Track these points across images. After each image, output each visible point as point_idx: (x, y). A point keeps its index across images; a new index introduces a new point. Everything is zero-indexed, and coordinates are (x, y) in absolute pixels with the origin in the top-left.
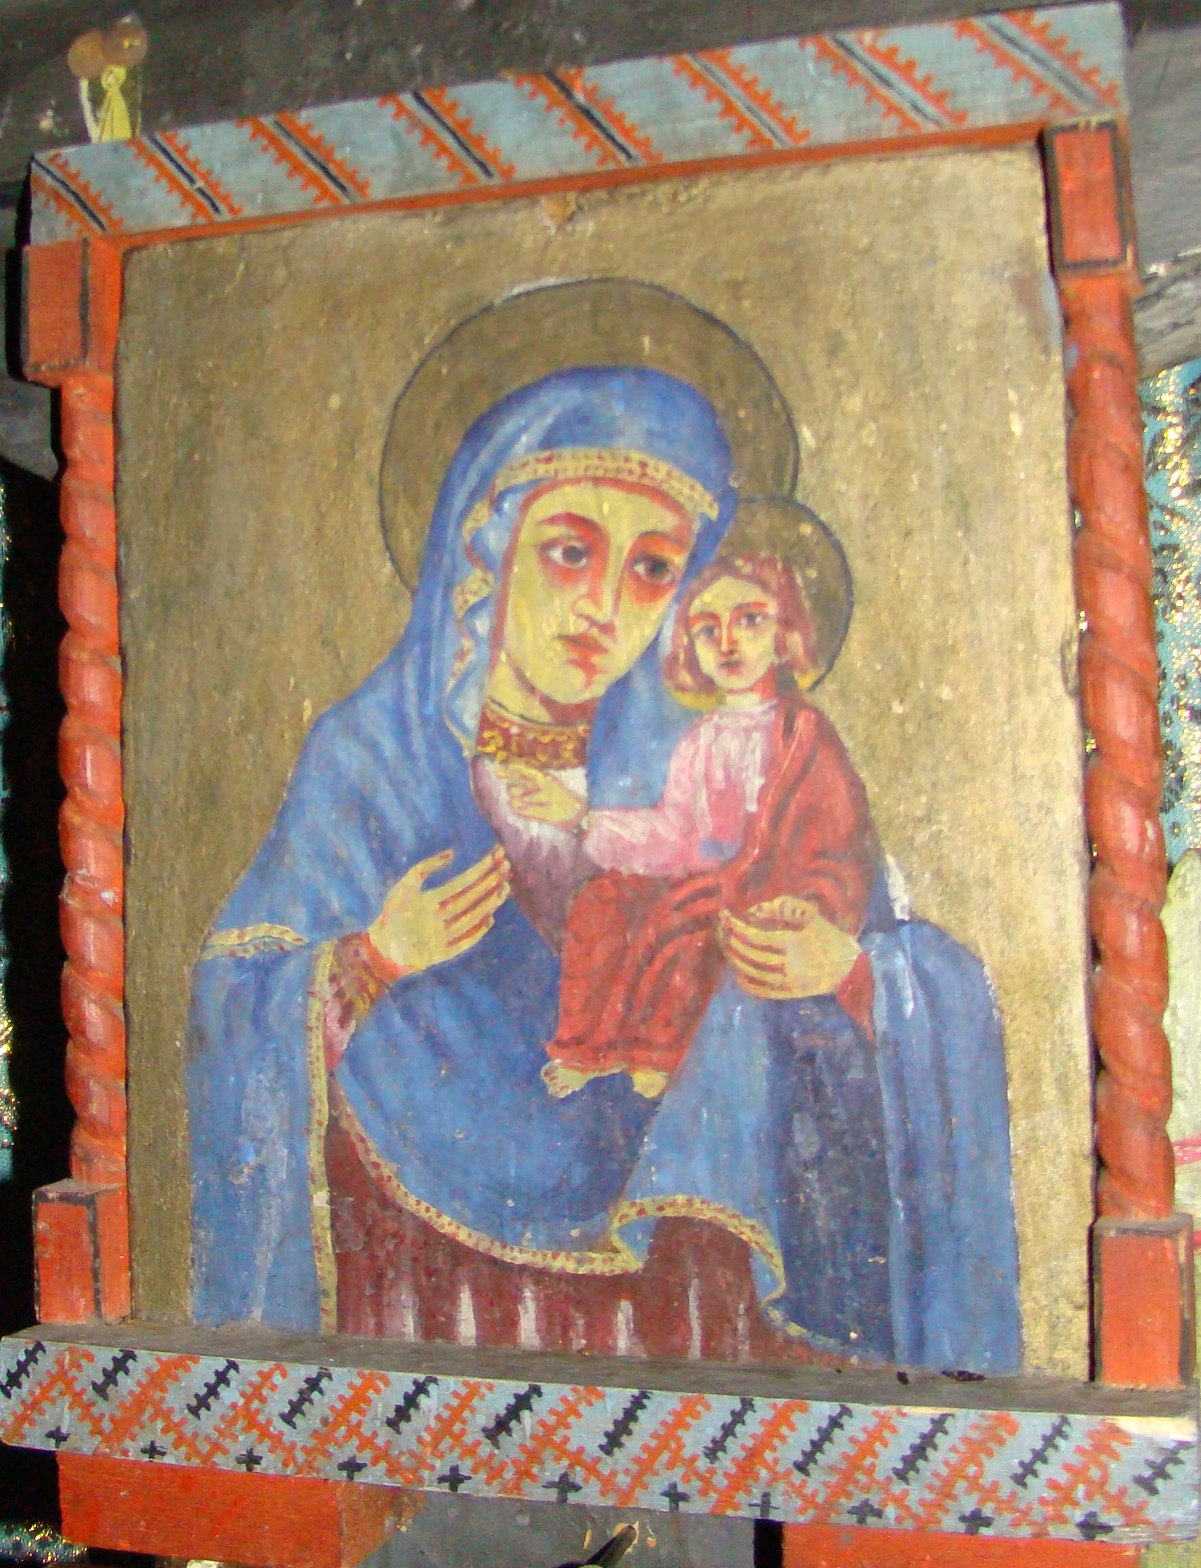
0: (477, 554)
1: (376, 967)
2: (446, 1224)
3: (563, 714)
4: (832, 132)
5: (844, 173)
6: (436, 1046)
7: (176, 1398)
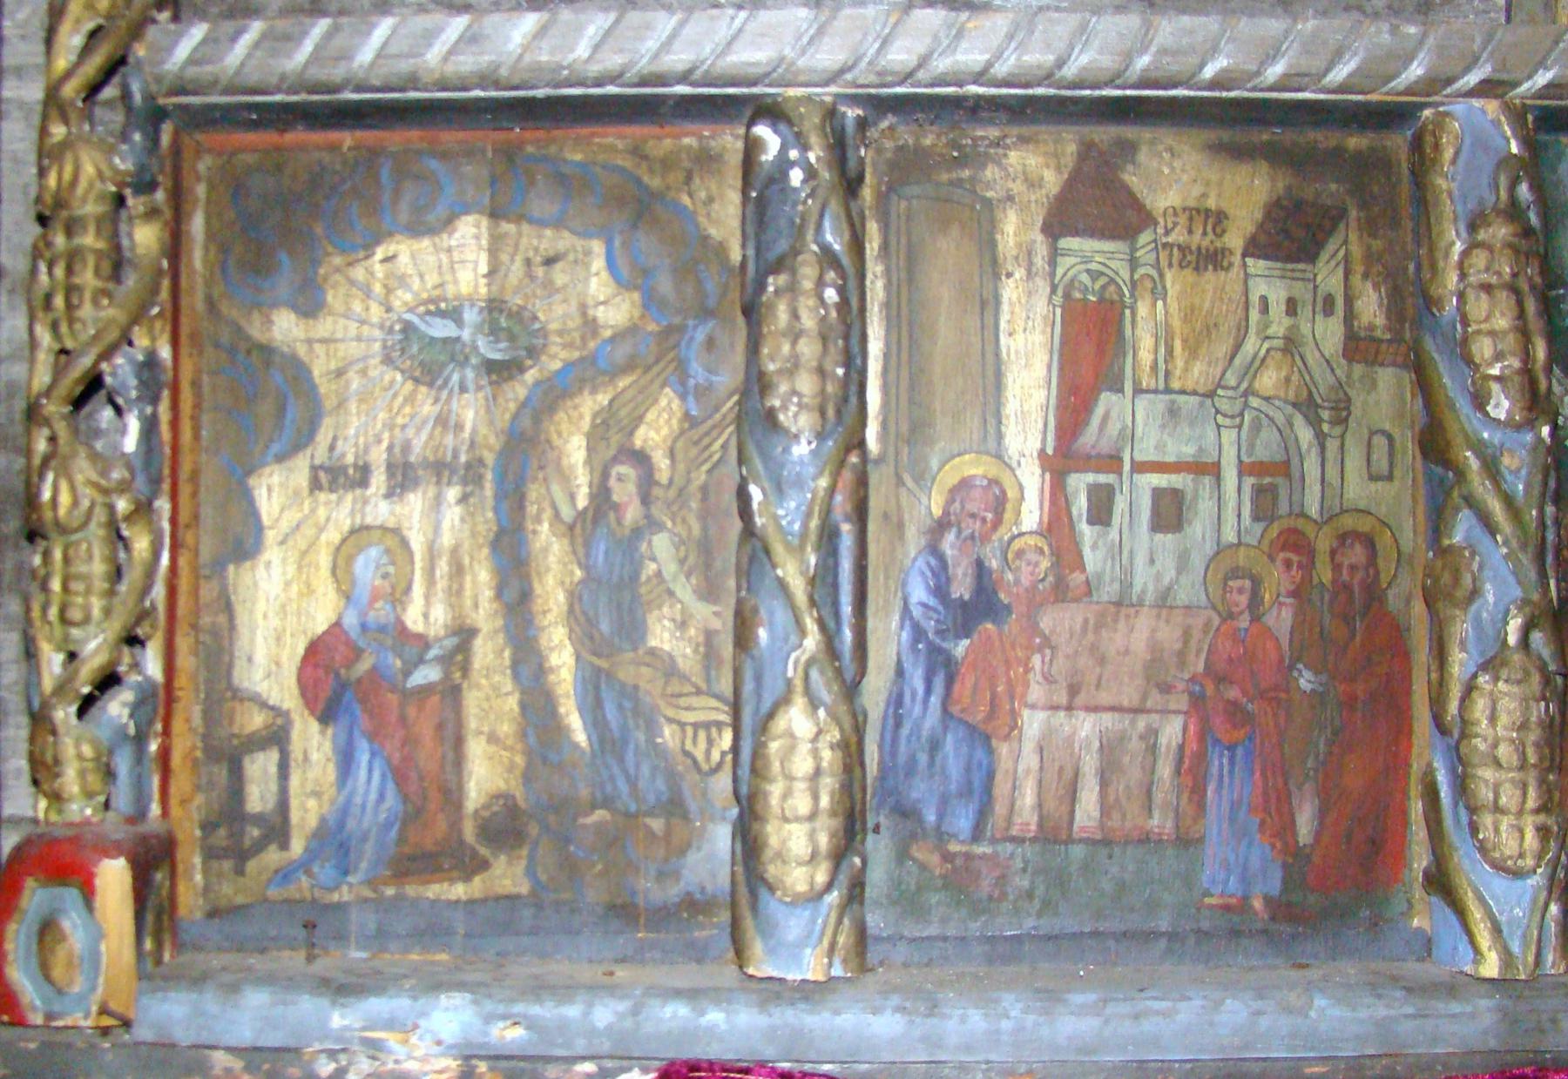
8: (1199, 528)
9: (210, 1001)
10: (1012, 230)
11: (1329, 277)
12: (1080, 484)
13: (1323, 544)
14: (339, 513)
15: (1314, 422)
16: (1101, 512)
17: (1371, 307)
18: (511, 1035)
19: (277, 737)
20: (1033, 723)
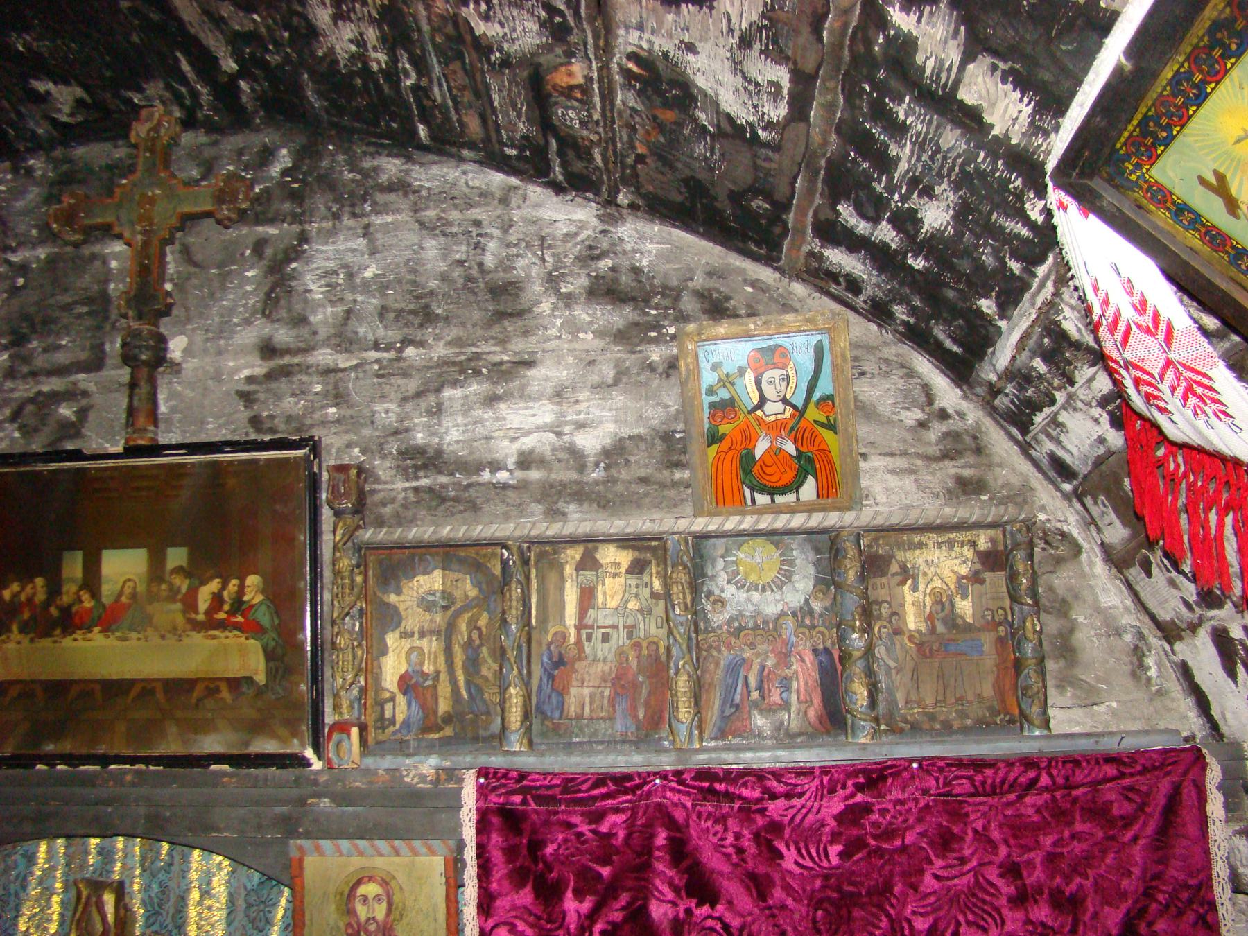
8: (613, 642)
9: (378, 759)
10: (569, 570)
11: (646, 578)
12: (584, 632)
13: (644, 645)
14: (407, 644)
15: (642, 614)
16: (589, 639)
17: (657, 585)
18: (447, 764)
19: (392, 699)
20: (573, 691)
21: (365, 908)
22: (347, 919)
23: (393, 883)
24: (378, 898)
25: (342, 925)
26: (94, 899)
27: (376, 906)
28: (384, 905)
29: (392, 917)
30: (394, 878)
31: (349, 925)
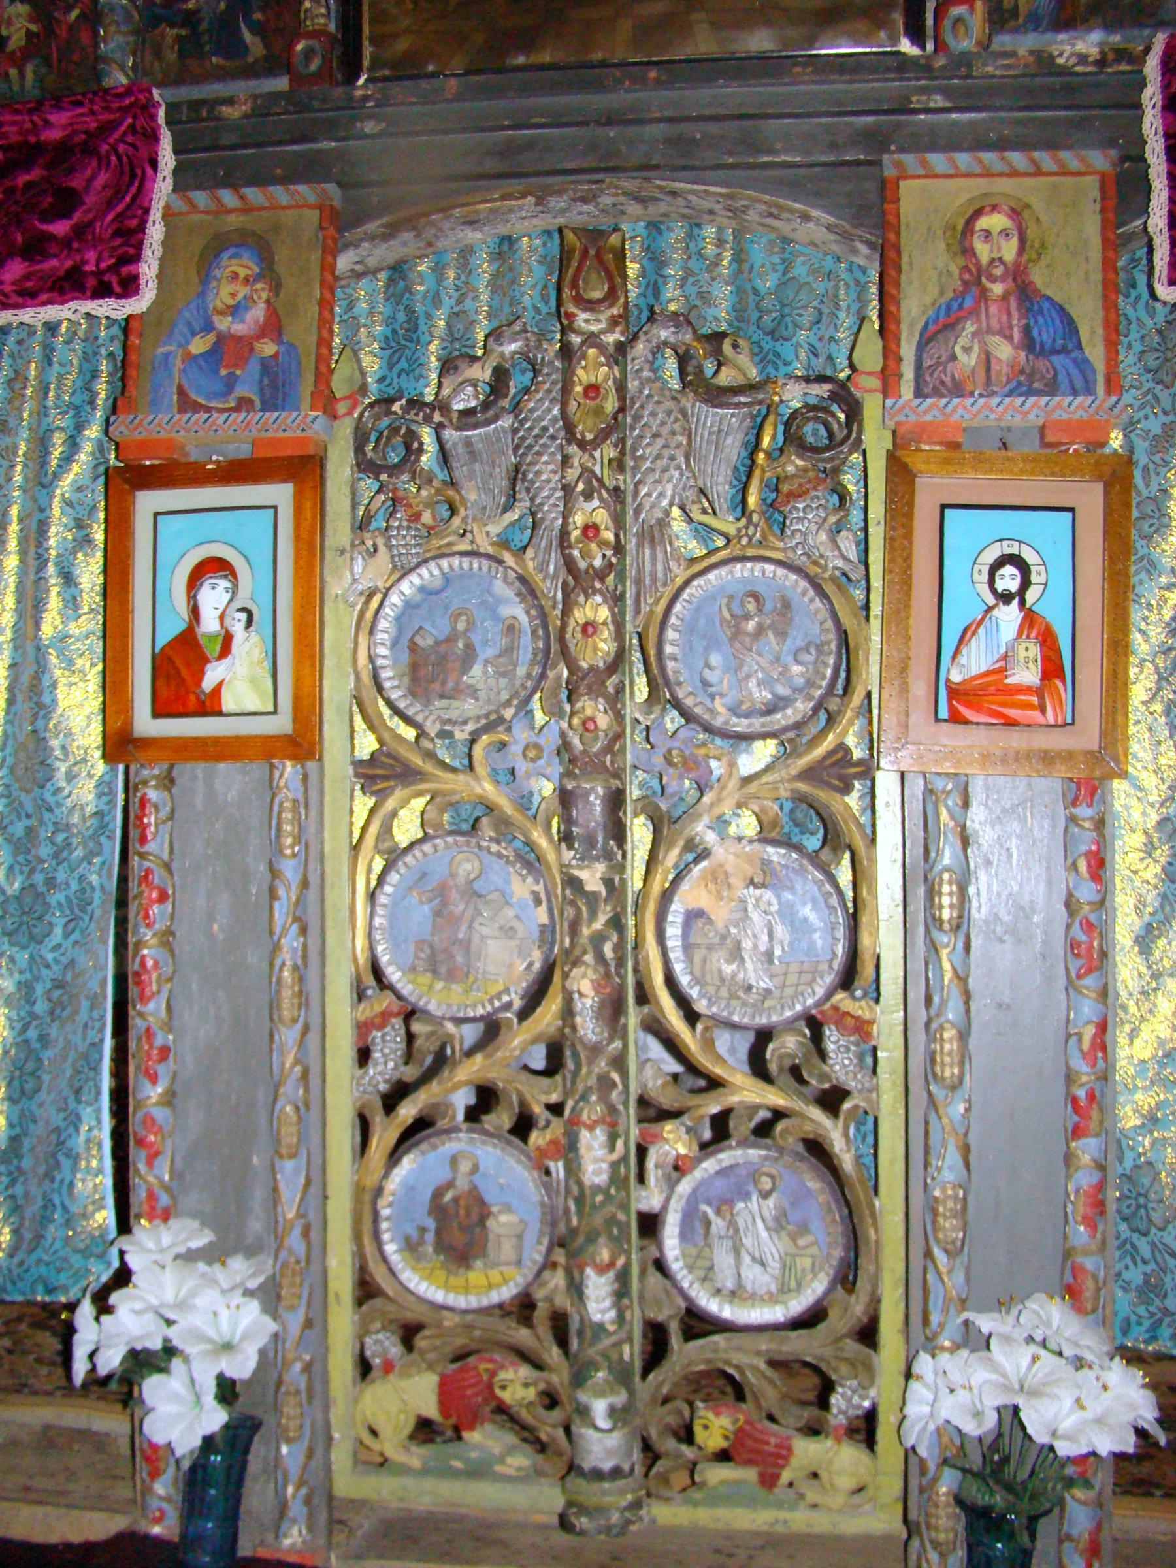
0: (215, 278)
1: (189, 353)
2: (200, 400)
3: (228, 307)
4: (284, 203)
5: (288, 212)
6: (200, 368)
7: (145, 423)
21: (987, 247)
22: (961, 261)
23: (1026, 214)
24: (1005, 233)
25: (956, 271)
26: (592, 252)
27: (1003, 243)
28: (1014, 242)
29: (1025, 257)
30: (1028, 206)
31: (965, 269)
